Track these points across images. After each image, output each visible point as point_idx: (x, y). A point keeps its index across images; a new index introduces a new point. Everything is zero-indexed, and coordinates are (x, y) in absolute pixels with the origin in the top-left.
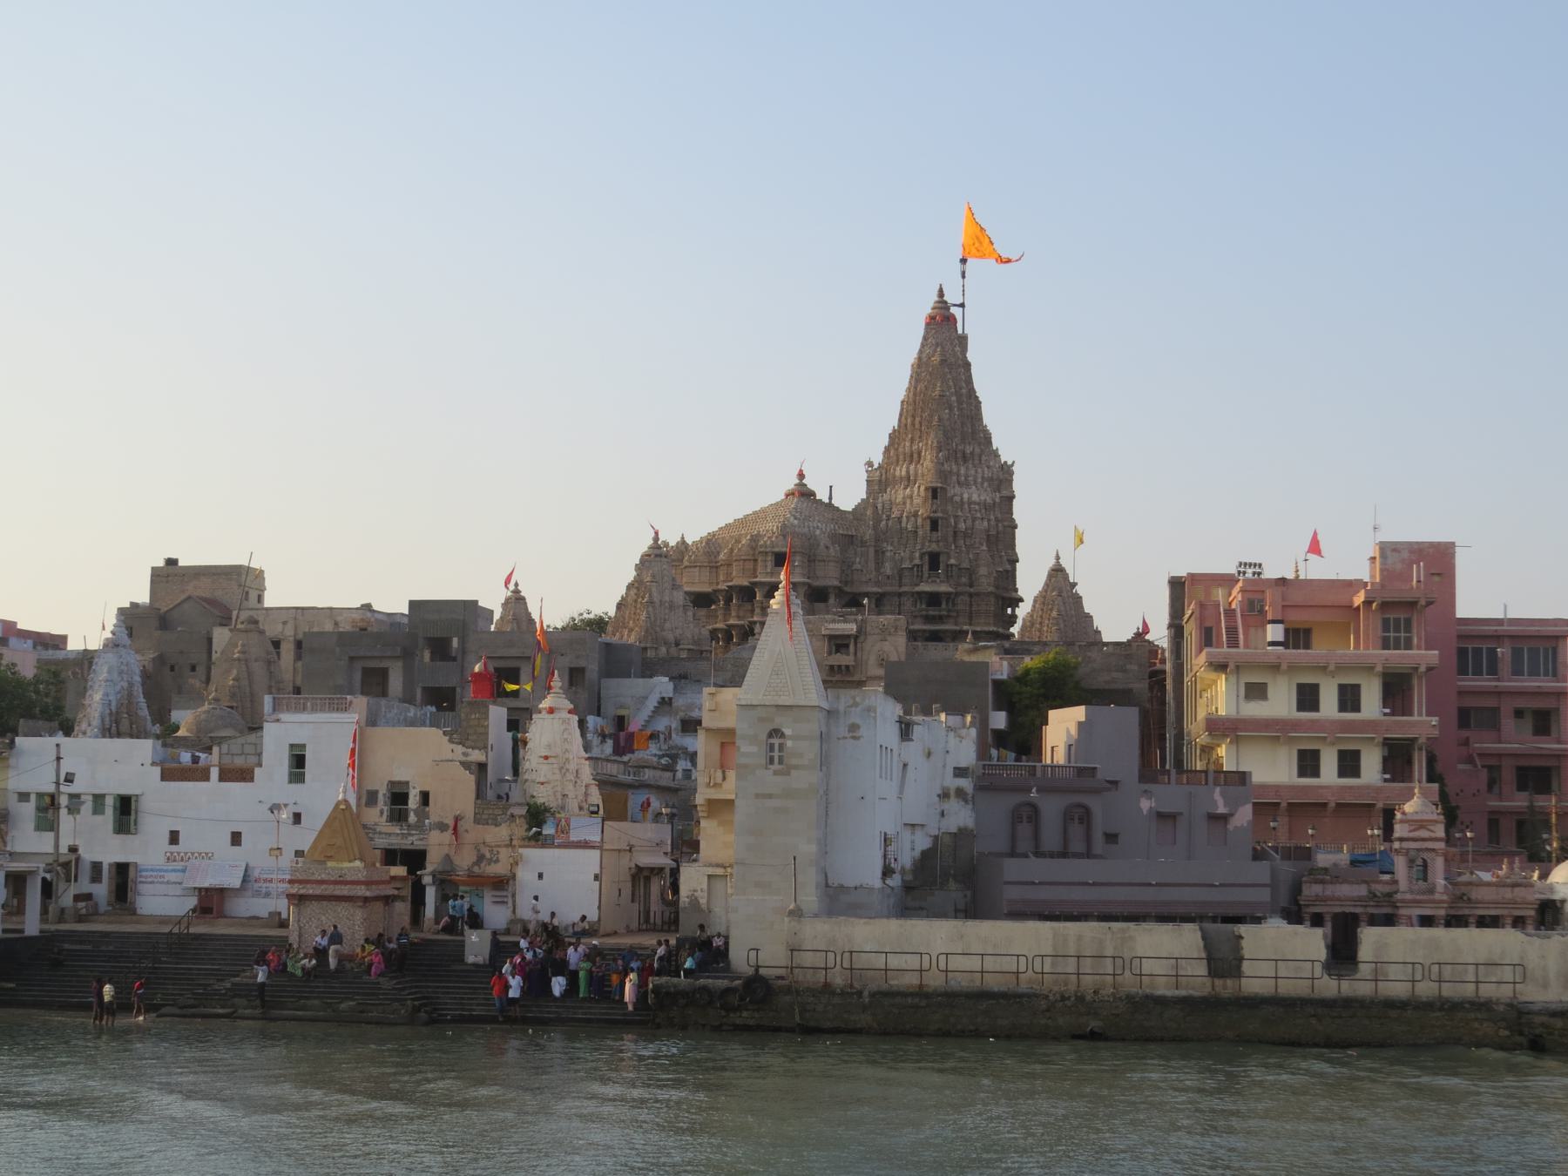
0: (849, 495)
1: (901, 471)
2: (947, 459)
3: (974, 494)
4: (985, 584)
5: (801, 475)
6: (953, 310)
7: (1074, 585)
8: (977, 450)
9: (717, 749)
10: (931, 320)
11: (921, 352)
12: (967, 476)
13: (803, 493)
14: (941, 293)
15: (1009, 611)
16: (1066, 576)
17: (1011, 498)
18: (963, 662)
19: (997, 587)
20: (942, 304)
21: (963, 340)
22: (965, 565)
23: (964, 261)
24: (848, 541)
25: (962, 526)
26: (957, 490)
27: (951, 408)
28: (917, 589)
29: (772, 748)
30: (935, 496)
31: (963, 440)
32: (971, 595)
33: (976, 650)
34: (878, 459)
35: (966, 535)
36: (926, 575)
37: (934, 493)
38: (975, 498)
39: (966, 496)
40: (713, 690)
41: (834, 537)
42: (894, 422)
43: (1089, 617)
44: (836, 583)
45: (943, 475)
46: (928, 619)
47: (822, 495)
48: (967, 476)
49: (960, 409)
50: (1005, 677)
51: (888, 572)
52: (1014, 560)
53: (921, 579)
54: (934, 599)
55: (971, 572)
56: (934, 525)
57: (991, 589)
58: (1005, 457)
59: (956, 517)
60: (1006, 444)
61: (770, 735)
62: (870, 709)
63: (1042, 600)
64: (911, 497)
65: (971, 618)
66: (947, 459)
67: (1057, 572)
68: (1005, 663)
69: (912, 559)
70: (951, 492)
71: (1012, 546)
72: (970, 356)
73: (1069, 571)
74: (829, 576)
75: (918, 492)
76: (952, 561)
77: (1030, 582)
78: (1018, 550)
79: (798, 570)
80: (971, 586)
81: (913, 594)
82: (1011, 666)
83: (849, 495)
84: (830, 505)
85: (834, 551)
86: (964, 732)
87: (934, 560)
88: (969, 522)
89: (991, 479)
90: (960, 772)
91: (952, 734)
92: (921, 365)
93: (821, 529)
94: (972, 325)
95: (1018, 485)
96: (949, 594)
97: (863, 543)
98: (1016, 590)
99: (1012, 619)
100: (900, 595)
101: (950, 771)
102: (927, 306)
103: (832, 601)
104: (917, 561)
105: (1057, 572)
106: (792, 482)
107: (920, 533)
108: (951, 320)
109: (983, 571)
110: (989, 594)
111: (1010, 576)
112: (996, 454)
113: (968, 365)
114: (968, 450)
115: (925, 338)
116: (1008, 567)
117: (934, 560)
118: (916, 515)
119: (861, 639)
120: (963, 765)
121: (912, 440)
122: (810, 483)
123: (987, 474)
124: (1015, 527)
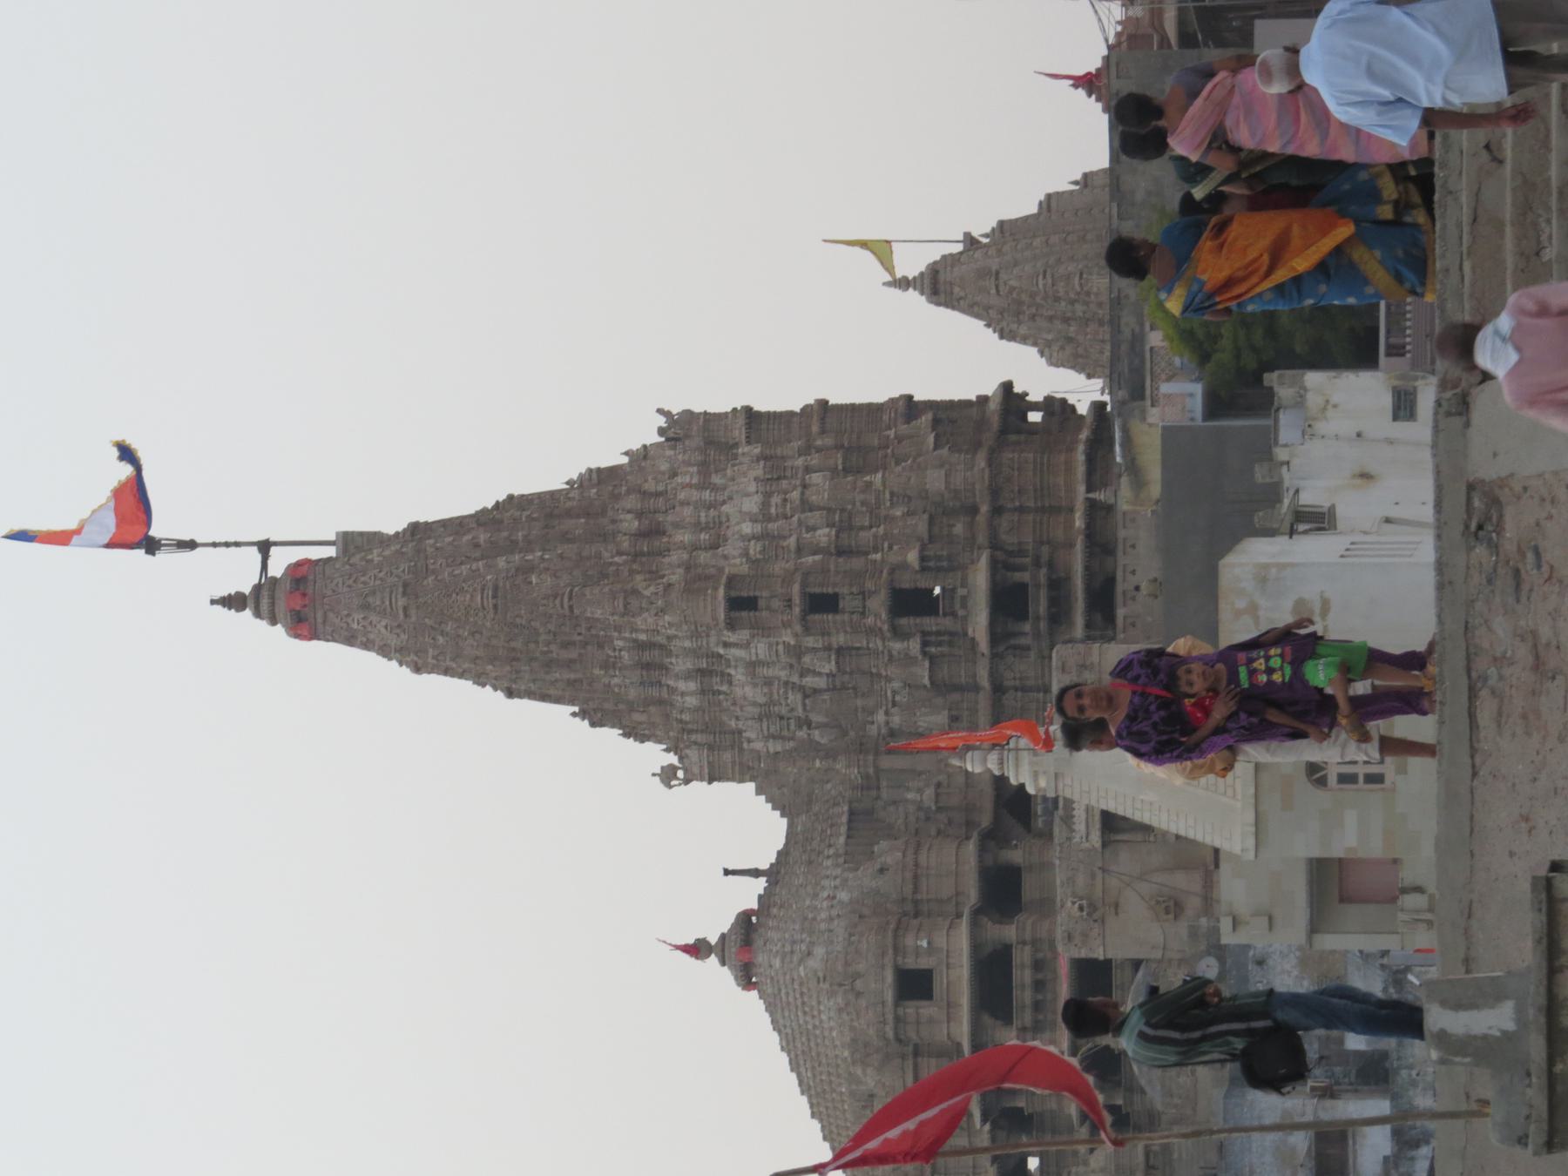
0: (742, 826)
1: (687, 694)
2: (654, 575)
3: (743, 502)
4: (973, 471)
5: (697, 949)
6: (277, 568)
7: (970, 241)
8: (632, 502)
9: (1352, 910)
10: (304, 625)
11: (384, 651)
12: (698, 527)
13: (741, 948)
14: (234, 602)
15: (1035, 417)
16: (949, 261)
17: (750, 416)
18: (1166, 484)
19: (977, 445)
20: (263, 600)
21: (350, 542)
22: (922, 526)
24: (864, 822)
25: (824, 535)
26: (732, 548)
27: (529, 569)
28: (983, 645)
29: (1345, 779)
30: (750, 604)
31: (605, 537)
32: (997, 511)
33: (1133, 468)
34: (656, 755)
35: (845, 526)
36: (947, 623)
38: (751, 505)
39: (747, 528)
40: (1225, 924)
41: (854, 856)
42: (560, 716)
43: (1050, 203)
44: (971, 847)
45: (697, 581)
46: (1059, 615)
47: (749, 894)
48: (698, 527)
49: (529, 546)
50: (1197, 389)
51: (942, 718)
52: (909, 407)
53: (957, 637)
54: (1008, 602)
55: (940, 512)
56: (821, 603)
57: (981, 461)
58: (647, 433)
59: (799, 550)
60: (615, 432)
61: (1322, 782)
62: (1263, 576)
63: (1010, 320)
64: (752, 666)
65: (1054, 510)
66: (654, 575)
67: (939, 284)
68: (1165, 388)
69: (908, 660)
70: (738, 566)
71: (870, 412)
72: (392, 523)
73: (935, 253)
74: (957, 867)
75: (744, 649)
76: (912, 557)
77: (965, 360)
78: (880, 397)
79: (941, 941)
80: (973, 510)
81: (995, 656)
82: (1169, 379)
83: (742, 826)
84: (774, 874)
85: (888, 852)
86: (1313, 400)
87: (910, 603)
88: (815, 518)
89: (705, 468)
90: (1404, 406)
91: (1321, 427)
92: (420, 654)
93: (837, 887)
94: (312, 521)
95: (720, 404)
96: (994, 565)
97: (869, 784)
98: (983, 400)
99: (1057, 408)
100: (998, 689)
101: (1403, 429)
102: (269, 639)
103: (1015, 856)
104: (914, 646)
105: (939, 284)
106: (716, 974)
107: (840, 639)
108: (301, 573)
109: (935, 480)
110: (990, 462)
111: (949, 419)
112: (641, 457)
113: (415, 529)
114: (630, 523)
115: (350, 640)
116: (926, 419)
117: (910, 603)
118: (797, 652)
120: (1387, 400)
121: (607, 665)
122: (716, 926)
123: (690, 475)
124: (823, 404)
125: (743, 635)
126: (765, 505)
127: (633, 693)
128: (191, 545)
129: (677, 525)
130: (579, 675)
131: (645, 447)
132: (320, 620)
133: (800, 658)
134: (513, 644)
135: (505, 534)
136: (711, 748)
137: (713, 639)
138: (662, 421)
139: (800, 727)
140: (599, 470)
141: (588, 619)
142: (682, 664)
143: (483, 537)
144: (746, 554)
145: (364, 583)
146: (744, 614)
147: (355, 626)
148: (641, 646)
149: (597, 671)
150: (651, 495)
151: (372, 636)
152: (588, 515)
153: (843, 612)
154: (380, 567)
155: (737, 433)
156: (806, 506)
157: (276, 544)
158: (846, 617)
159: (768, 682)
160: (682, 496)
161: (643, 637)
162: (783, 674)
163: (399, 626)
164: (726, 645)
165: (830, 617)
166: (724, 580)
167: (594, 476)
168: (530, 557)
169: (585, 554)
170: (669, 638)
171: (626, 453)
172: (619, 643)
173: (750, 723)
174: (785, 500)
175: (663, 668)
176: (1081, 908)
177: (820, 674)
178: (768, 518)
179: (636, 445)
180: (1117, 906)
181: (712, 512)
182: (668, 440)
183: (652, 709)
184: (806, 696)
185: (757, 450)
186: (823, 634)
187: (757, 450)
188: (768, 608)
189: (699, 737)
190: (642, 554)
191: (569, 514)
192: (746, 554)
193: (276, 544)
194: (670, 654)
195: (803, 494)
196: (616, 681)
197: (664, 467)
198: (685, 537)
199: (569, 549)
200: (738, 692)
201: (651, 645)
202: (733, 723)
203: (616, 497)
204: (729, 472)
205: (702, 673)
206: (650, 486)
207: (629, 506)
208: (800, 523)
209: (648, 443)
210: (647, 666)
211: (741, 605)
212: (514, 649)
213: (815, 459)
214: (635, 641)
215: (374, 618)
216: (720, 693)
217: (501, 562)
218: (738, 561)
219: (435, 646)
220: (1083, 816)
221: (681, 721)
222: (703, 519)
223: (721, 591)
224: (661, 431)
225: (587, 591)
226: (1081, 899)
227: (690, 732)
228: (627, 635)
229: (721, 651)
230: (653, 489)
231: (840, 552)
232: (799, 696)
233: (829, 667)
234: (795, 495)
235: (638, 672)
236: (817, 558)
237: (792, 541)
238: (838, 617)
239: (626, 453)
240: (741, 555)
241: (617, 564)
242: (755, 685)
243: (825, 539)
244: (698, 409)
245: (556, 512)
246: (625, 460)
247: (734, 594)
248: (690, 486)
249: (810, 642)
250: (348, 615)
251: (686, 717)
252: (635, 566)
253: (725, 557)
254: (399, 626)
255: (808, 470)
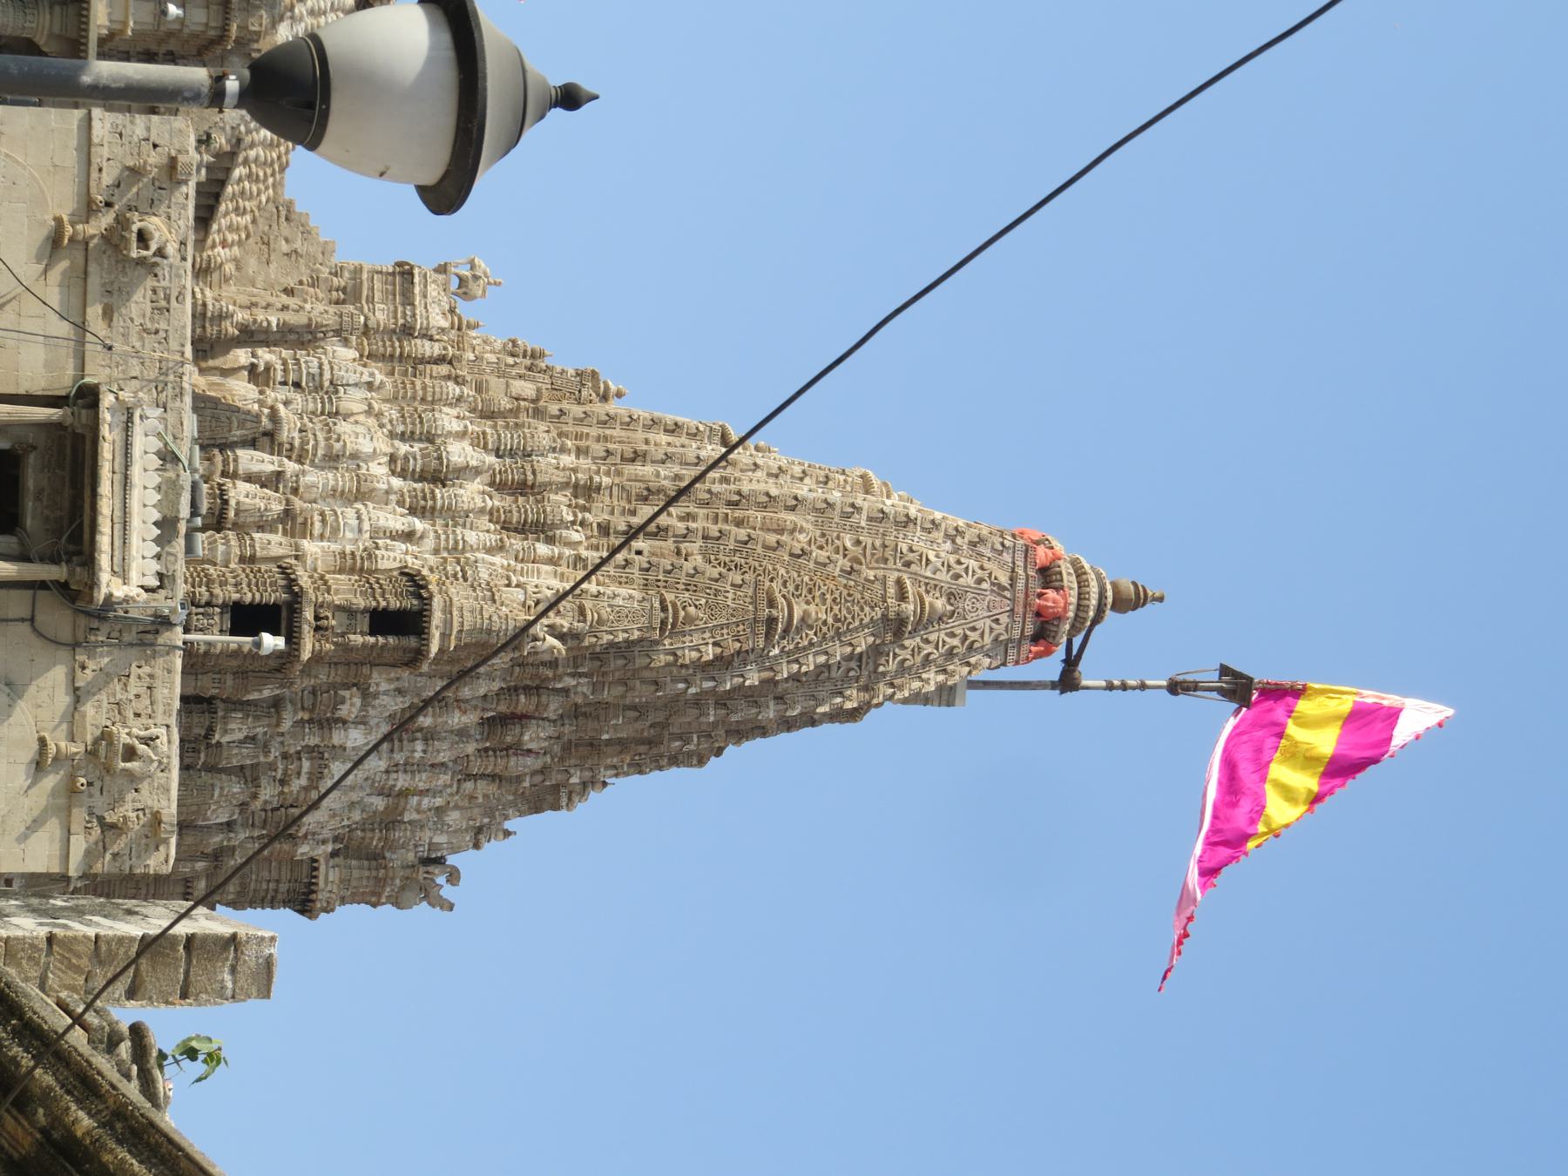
8: (518, 765)
12: (429, 736)
23: (1237, 687)
30: (382, 621)
31: (576, 713)
37: (401, 622)
39: (356, 738)
48: (429, 736)
49: (698, 702)
59: (276, 704)
64: (361, 494)
88: (241, 756)
89: (390, 821)
114: (534, 736)
119: (57, 618)
121: (586, 491)
125: (393, 556)
126: (316, 776)
127: (542, 435)
128: (1175, 687)
129: (462, 733)
130: (629, 469)
131: (477, 846)
132: (1021, 571)
133: (287, 512)
134: (742, 533)
135: (734, 718)
136: (407, 331)
137: (429, 543)
138: (447, 892)
139: (268, 367)
140: (556, 807)
141: (629, 582)
142: (471, 493)
143: (771, 712)
144: (367, 695)
145: (952, 635)
146: (395, 604)
147: (973, 564)
148: (541, 529)
149: (606, 481)
150: (483, 776)
151: (948, 546)
152: (594, 745)
153: (224, 606)
154: (927, 661)
155: (334, 875)
156: (249, 775)
157: (1053, 685)
158: (220, 594)
159: (332, 459)
160: (445, 778)
161: (543, 549)
162: (314, 478)
163: (908, 564)
164: (409, 536)
165: (248, 598)
166: (425, 668)
167: (564, 801)
168: (708, 685)
169: (620, 689)
170: (501, 548)
171: (507, 834)
172: (576, 535)
173: (353, 378)
174: (283, 782)
175: (499, 485)
176: (143, 238)
177: (250, 478)
178: (315, 753)
179: (492, 847)
180: (55, 242)
181: (399, 757)
182: (440, 861)
183: (506, 404)
184: (270, 435)
185: (304, 850)
186: (252, 559)
187: (304, 850)
188: (348, 611)
189: (428, 349)
190: (527, 689)
191: (622, 745)
192: (367, 695)
193: (1053, 685)
194: (492, 514)
195: (255, 796)
196: (568, 460)
197: (453, 817)
198: (457, 719)
199: (641, 693)
200: (384, 446)
201: (522, 529)
202: (379, 377)
203: (543, 771)
204: (357, 816)
205: (437, 476)
206: (483, 787)
207: (529, 761)
208: (266, 749)
209: (472, 852)
210: (522, 488)
211: (401, 622)
212: (739, 523)
213: (217, 839)
214: (550, 540)
215: (943, 576)
216: (403, 437)
217: (753, 678)
218: (384, 686)
219: (856, 529)
220: (136, 471)
221: (458, 380)
222: (419, 746)
223: (434, 647)
224: (454, 877)
225: (636, 635)
226: (141, 262)
227: (441, 360)
228: (567, 552)
229: (419, 525)
230: (481, 784)
231: (210, 701)
232: (284, 436)
233: (240, 493)
234: (268, 792)
235: (540, 479)
236: (254, 696)
237: (286, 725)
238: (235, 596)
239: (507, 834)
240: (376, 696)
241: (573, 675)
242: (355, 456)
243: (232, 726)
244: (387, 910)
245: (643, 749)
246: (508, 825)
247: (412, 642)
248: (423, 793)
249: (273, 543)
250: (980, 581)
251: (453, 389)
252: (550, 673)
253: (400, 691)
254: (908, 564)
255: (229, 826)
